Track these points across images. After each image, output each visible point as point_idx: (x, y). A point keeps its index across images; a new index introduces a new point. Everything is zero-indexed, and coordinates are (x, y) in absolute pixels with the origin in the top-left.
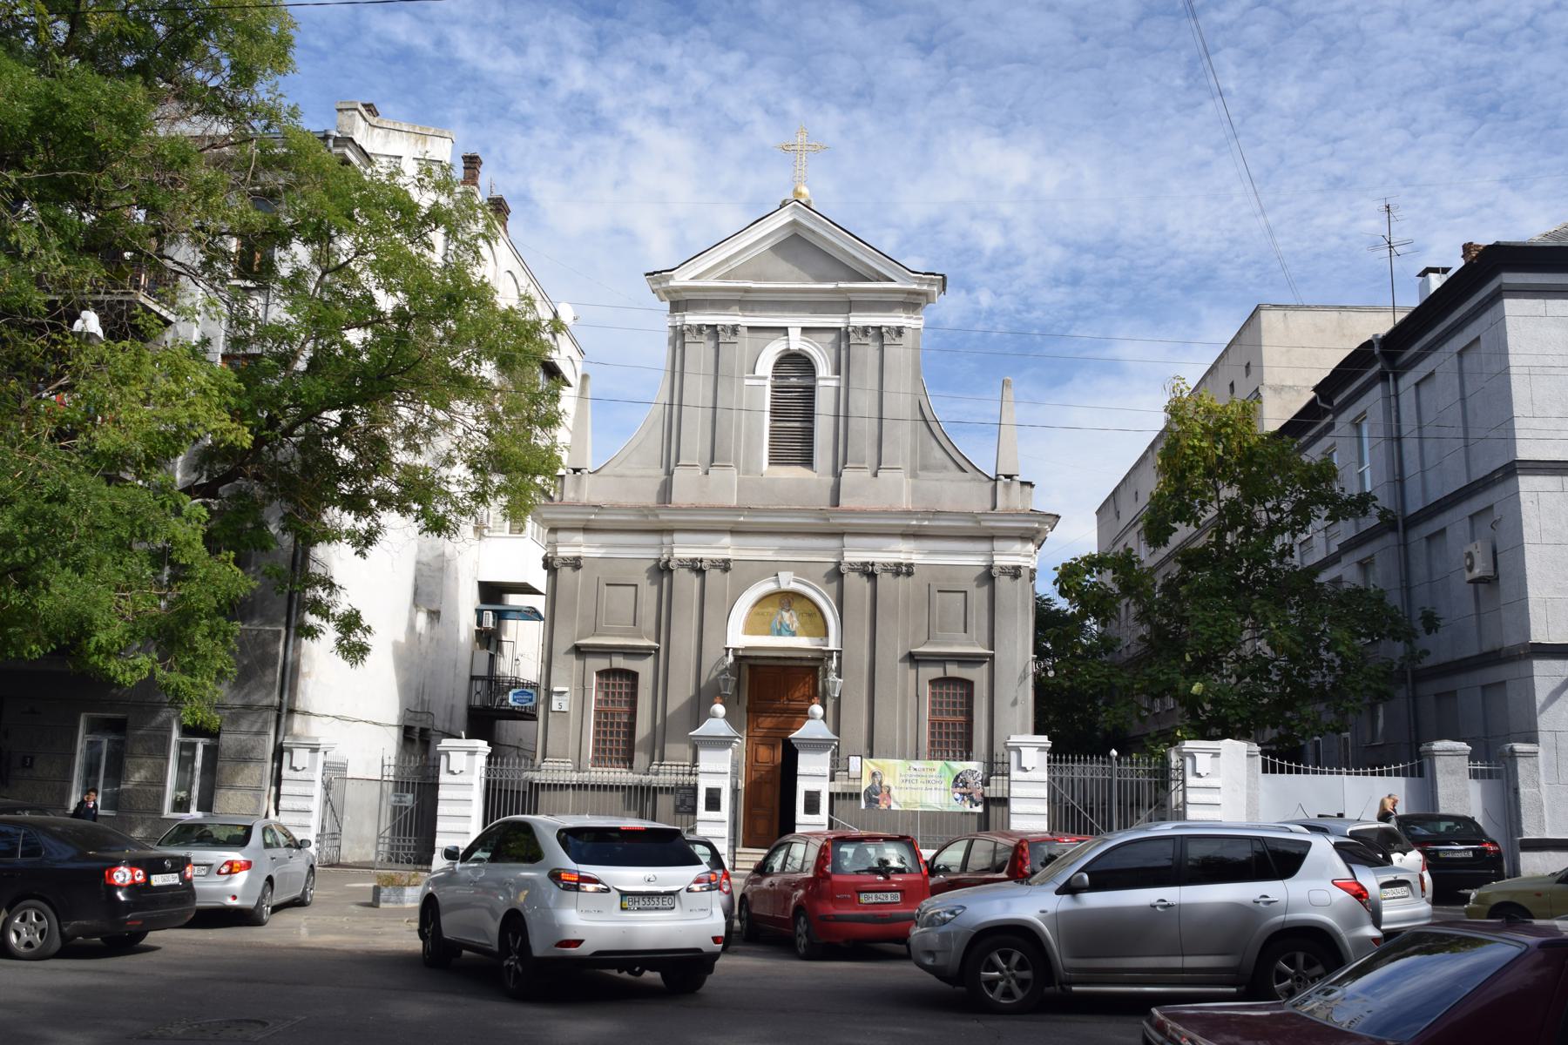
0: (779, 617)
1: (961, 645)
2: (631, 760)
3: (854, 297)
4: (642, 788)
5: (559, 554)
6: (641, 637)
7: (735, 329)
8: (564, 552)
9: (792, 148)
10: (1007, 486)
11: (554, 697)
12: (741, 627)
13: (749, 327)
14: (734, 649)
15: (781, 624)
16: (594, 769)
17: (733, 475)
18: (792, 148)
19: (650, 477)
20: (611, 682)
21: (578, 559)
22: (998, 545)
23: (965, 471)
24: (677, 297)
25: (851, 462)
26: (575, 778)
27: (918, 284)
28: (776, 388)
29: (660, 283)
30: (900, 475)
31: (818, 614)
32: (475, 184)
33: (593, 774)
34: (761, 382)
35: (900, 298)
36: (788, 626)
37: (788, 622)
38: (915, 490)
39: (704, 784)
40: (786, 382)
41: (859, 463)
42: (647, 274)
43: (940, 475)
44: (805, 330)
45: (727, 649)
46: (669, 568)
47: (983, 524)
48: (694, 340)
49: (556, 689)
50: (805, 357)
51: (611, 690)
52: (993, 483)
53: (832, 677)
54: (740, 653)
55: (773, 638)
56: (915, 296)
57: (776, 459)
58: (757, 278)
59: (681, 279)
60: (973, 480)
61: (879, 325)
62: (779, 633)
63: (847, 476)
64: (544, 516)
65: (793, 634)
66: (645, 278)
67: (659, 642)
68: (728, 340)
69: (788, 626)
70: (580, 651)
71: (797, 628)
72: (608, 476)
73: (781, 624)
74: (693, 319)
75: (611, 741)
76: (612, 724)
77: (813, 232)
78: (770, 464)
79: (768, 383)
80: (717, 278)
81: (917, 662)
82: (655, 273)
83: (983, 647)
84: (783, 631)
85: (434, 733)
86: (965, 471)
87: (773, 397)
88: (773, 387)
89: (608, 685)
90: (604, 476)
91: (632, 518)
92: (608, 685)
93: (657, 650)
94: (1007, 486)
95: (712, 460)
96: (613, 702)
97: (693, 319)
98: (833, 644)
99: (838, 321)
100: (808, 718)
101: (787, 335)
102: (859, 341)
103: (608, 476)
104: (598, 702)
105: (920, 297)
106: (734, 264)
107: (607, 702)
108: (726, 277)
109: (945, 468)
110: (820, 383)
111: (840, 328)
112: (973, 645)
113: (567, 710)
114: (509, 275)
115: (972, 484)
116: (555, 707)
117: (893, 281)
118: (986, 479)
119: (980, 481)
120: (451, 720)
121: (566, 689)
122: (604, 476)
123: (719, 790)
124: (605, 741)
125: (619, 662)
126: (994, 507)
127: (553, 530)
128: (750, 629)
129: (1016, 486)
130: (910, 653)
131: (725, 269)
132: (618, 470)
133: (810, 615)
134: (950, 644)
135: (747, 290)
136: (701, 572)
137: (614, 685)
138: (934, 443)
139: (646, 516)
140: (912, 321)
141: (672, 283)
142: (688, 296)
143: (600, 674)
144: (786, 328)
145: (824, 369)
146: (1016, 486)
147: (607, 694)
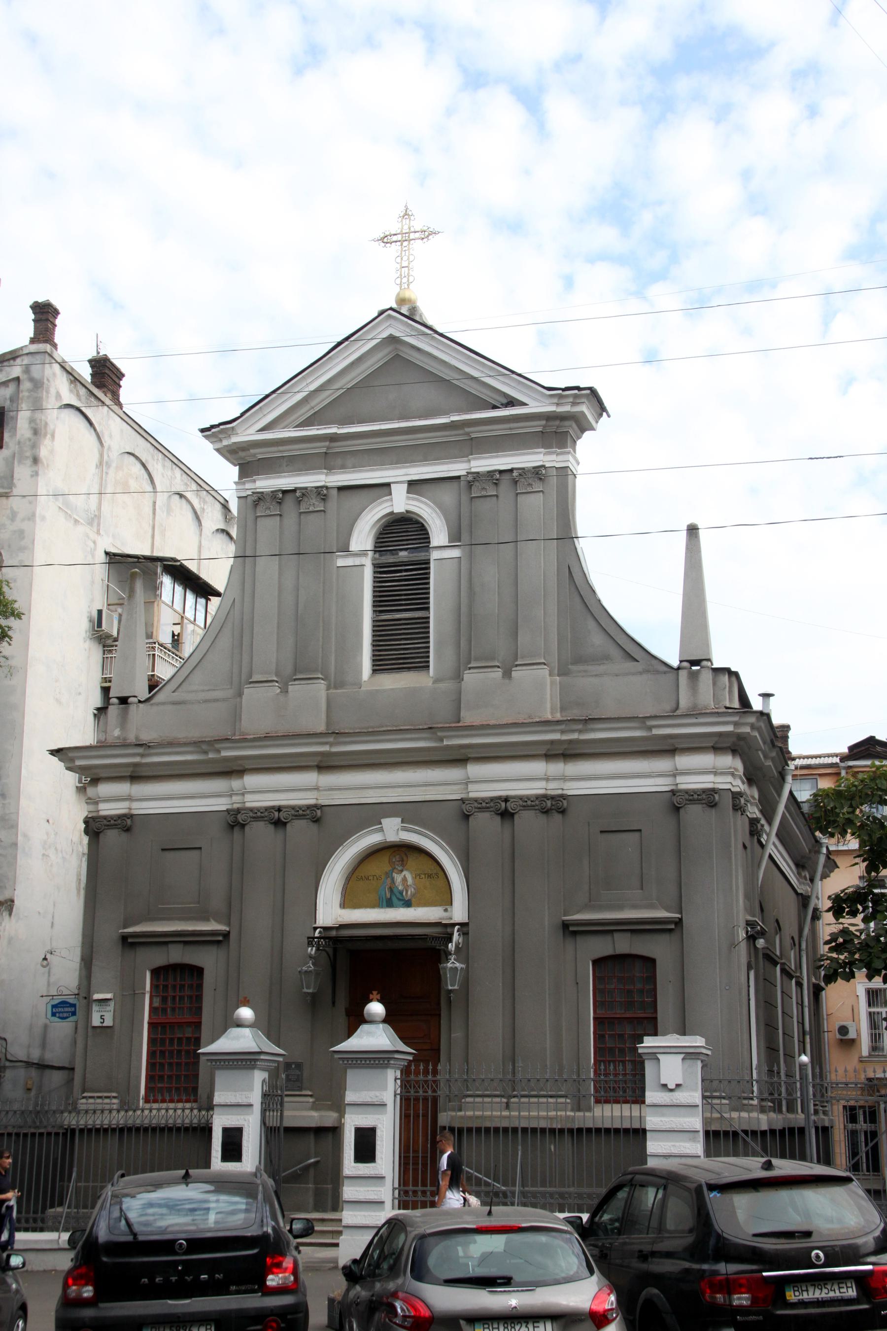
0: (389, 881)
1: (635, 907)
2: (195, 1089)
3: (476, 432)
4: (73, 1131)
5: (102, 813)
6: (205, 919)
7: (321, 493)
8: (108, 809)
9: (395, 238)
10: (694, 676)
11: (95, 1008)
12: (337, 898)
13: (341, 489)
14: (326, 929)
15: (391, 891)
16: (148, 1106)
17: (319, 689)
18: (395, 238)
19: (216, 700)
20: (171, 981)
21: (131, 816)
22: (684, 761)
23: (638, 661)
24: (247, 456)
25: (476, 659)
26: (118, 1119)
27: (558, 404)
28: (379, 568)
29: (221, 440)
30: (544, 672)
31: (441, 873)
32: (46, 341)
33: (139, 1112)
34: (357, 561)
35: (536, 427)
36: (401, 893)
37: (400, 888)
38: (564, 689)
39: (220, 1122)
40: (390, 559)
41: (487, 659)
42: (203, 431)
43: (601, 669)
44: (414, 486)
45: (315, 929)
46: (239, 823)
47: (655, 732)
48: (268, 512)
49: (97, 996)
50: (418, 522)
51: (171, 993)
52: (671, 676)
53: (452, 963)
54: (334, 933)
55: (382, 910)
56: (557, 423)
57: (380, 665)
58: (343, 422)
59: (248, 434)
60: (646, 671)
61: (509, 467)
62: (390, 904)
63: (470, 677)
64: (78, 763)
65: (408, 904)
66: (200, 434)
67: (229, 924)
68: (311, 509)
69: (401, 893)
70: (128, 942)
71: (413, 895)
72: (163, 704)
73: (391, 891)
74: (267, 484)
75: (170, 1064)
76: (172, 1040)
77: (418, 350)
78: (375, 671)
79: (367, 563)
80: (296, 427)
81: (575, 933)
82: (213, 427)
83: (668, 910)
84: (394, 899)
85: (8, 1064)
86: (638, 661)
87: (376, 580)
88: (375, 566)
89: (166, 987)
90: (158, 704)
91: (189, 757)
92: (166, 987)
93: (226, 935)
94: (694, 676)
95: (296, 671)
96: (173, 1009)
97: (267, 484)
98: (459, 912)
99: (457, 468)
100: (365, 1022)
101: (390, 494)
102: (484, 493)
103: (163, 704)
104: (152, 1009)
105: (567, 423)
106: (319, 403)
107: (164, 1010)
108: (308, 423)
109: (606, 658)
110: (435, 555)
111: (458, 477)
112: (651, 907)
113: (111, 1024)
114: (132, 458)
115: (645, 677)
116: (96, 1021)
117: (525, 404)
118: (665, 669)
119: (657, 672)
120: (43, 1045)
121: (109, 996)
122: (158, 704)
123: (239, 1130)
124: (162, 1065)
125: (176, 955)
126: (677, 708)
127: (95, 781)
128: (348, 900)
129: (706, 677)
130: (563, 921)
131: (305, 413)
132: (177, 696)
133: (430, 876)
134: (620, 908)
135: (333, 438)
136: (279, 824)
137: (174, 987)
138: (591, 624)
139: (206, 753)
140: (554, 457)
141: (235, 439)
142: (260, 453)
143: (156, 973)
144: (388, 485)
145: (439, 535)
146: (706, 677)
147: (164, 999)
